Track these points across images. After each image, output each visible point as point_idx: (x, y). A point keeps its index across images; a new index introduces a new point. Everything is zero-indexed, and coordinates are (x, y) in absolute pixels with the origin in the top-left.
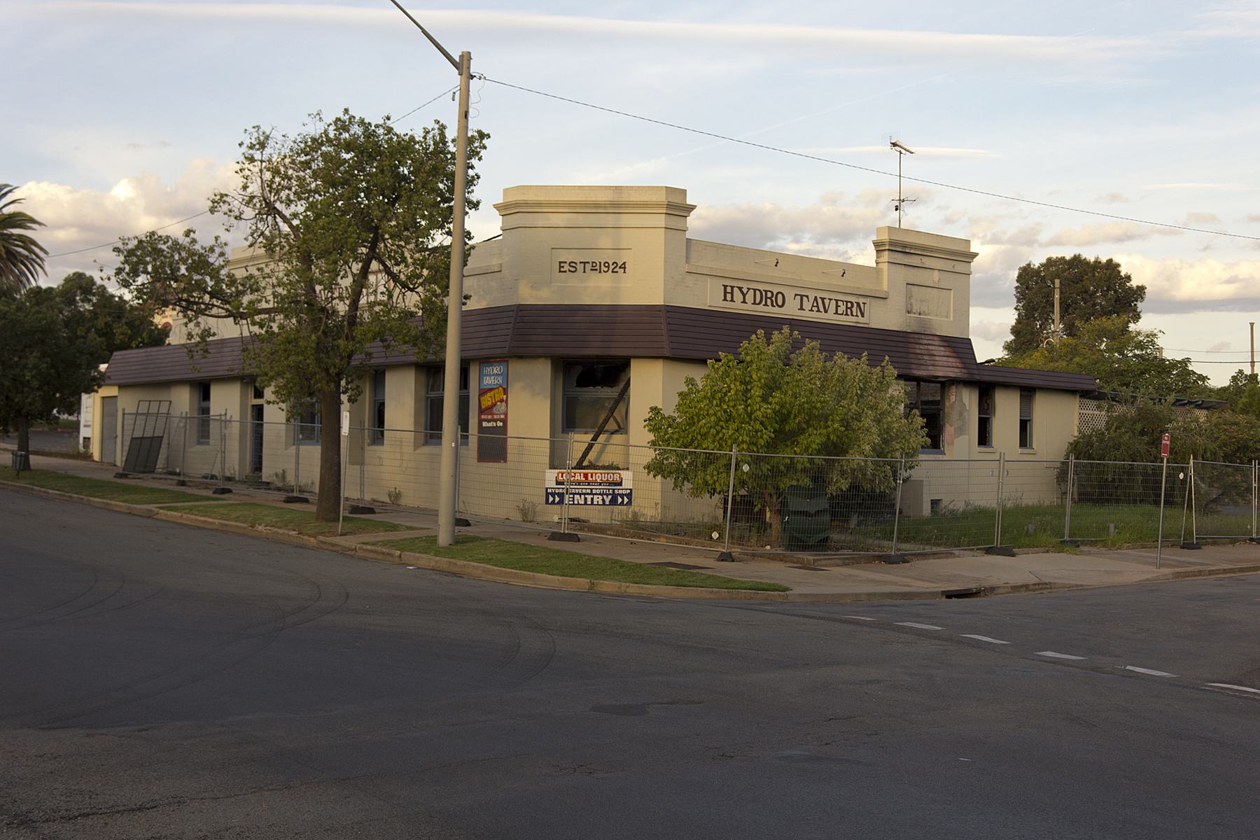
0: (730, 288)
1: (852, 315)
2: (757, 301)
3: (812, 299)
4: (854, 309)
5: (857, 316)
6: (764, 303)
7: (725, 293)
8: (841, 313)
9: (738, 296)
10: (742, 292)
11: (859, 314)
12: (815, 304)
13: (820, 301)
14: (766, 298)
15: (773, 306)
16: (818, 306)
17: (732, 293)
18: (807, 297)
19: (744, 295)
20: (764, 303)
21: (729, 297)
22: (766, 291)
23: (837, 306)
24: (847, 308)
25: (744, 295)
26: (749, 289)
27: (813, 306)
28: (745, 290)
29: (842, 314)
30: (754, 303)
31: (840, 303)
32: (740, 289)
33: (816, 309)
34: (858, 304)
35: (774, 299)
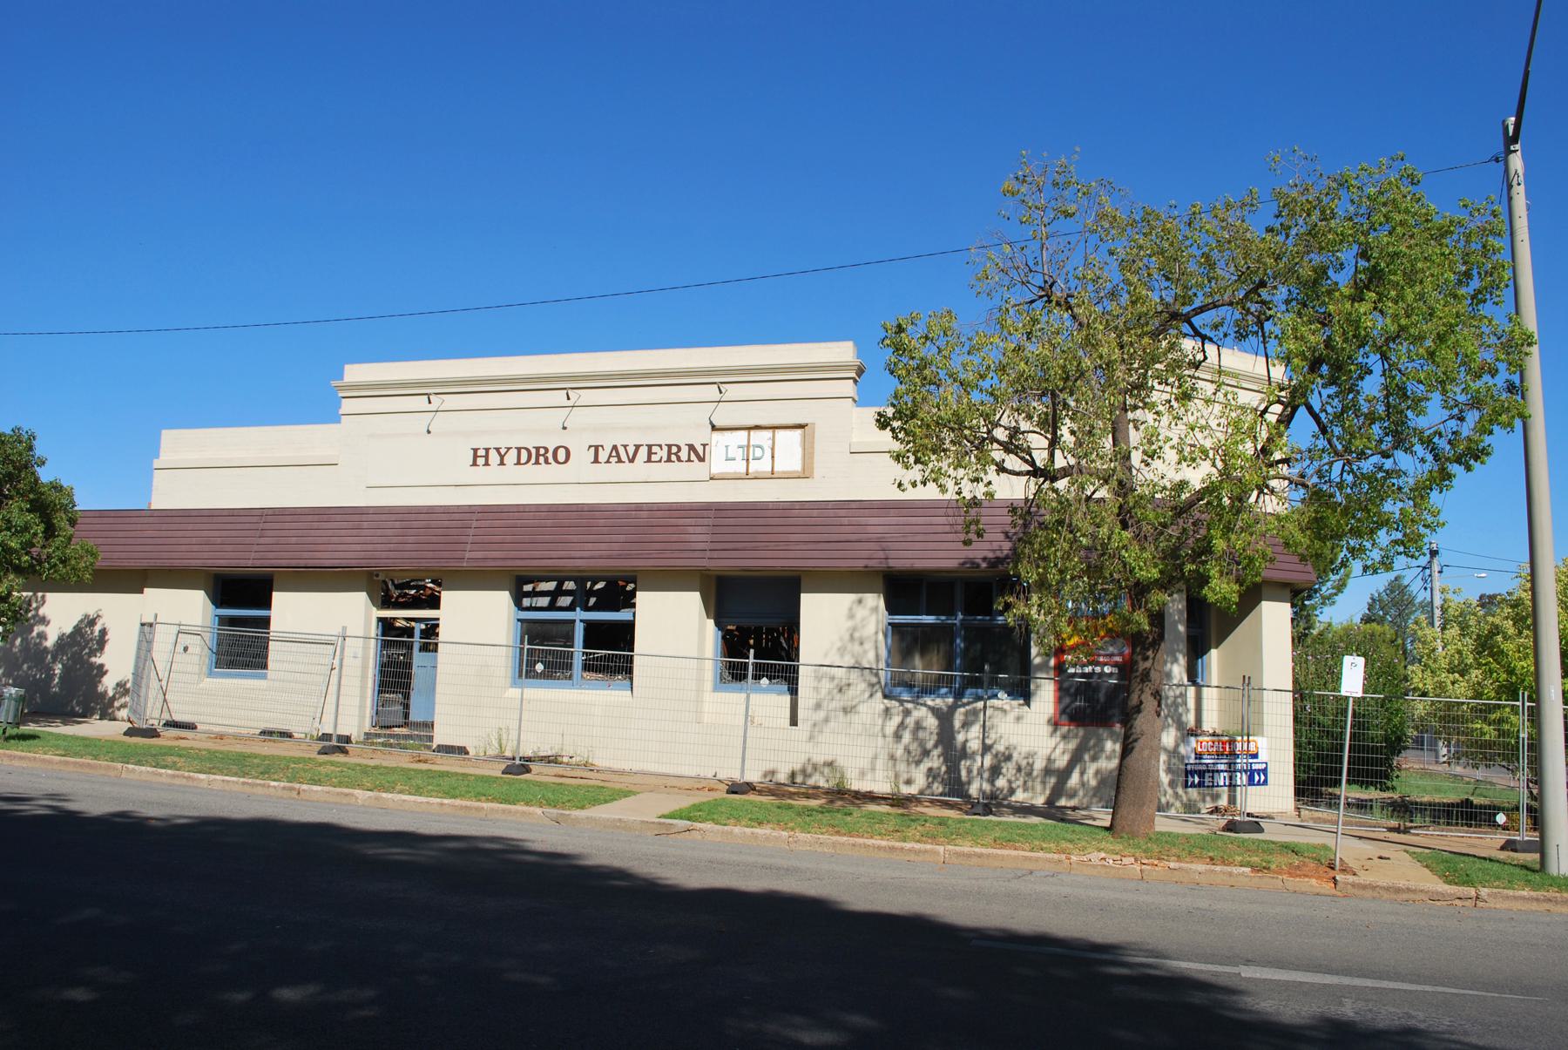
0: (484, 451)
1: (679, 459)
2: (523, 461)
3: (608, 449)
4: (684, 454)
5: (689, 460)
6: (533, 460)
7: (475, 457)
8: (658, 459)
9: (493, 454)
10: (499, 453)
11: (693, 457)
12: (614, 454)
13: (621, 450)
14: (538, 455)
15: (547, 462)
16: (618, 456)
17: (487, 457)
18: (602, 446)
19: (502, 457)
20: (533, 460)
21: (481, 461)
22: (537, 449)
23: (650, 453)
24: (670, 453)
25: (502, 457)
26: (509, 449)
27: (610, 456)
28: (503, 451)
29: (660, 461)
30: (518, 463)
31: (655, 449)
32: (498, 450)
33: (616, 459)
34: (691, 448)
35: (550, 455)
